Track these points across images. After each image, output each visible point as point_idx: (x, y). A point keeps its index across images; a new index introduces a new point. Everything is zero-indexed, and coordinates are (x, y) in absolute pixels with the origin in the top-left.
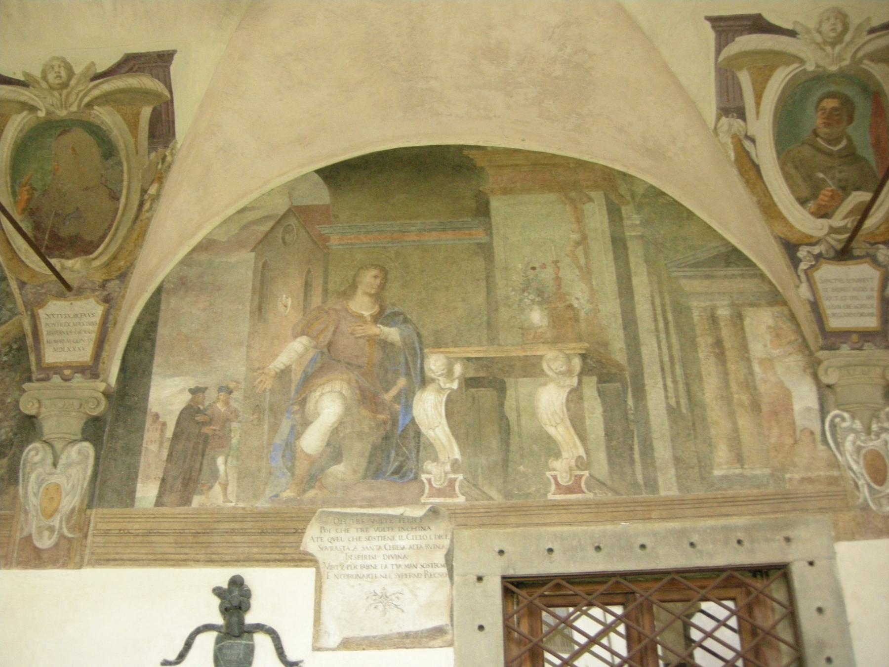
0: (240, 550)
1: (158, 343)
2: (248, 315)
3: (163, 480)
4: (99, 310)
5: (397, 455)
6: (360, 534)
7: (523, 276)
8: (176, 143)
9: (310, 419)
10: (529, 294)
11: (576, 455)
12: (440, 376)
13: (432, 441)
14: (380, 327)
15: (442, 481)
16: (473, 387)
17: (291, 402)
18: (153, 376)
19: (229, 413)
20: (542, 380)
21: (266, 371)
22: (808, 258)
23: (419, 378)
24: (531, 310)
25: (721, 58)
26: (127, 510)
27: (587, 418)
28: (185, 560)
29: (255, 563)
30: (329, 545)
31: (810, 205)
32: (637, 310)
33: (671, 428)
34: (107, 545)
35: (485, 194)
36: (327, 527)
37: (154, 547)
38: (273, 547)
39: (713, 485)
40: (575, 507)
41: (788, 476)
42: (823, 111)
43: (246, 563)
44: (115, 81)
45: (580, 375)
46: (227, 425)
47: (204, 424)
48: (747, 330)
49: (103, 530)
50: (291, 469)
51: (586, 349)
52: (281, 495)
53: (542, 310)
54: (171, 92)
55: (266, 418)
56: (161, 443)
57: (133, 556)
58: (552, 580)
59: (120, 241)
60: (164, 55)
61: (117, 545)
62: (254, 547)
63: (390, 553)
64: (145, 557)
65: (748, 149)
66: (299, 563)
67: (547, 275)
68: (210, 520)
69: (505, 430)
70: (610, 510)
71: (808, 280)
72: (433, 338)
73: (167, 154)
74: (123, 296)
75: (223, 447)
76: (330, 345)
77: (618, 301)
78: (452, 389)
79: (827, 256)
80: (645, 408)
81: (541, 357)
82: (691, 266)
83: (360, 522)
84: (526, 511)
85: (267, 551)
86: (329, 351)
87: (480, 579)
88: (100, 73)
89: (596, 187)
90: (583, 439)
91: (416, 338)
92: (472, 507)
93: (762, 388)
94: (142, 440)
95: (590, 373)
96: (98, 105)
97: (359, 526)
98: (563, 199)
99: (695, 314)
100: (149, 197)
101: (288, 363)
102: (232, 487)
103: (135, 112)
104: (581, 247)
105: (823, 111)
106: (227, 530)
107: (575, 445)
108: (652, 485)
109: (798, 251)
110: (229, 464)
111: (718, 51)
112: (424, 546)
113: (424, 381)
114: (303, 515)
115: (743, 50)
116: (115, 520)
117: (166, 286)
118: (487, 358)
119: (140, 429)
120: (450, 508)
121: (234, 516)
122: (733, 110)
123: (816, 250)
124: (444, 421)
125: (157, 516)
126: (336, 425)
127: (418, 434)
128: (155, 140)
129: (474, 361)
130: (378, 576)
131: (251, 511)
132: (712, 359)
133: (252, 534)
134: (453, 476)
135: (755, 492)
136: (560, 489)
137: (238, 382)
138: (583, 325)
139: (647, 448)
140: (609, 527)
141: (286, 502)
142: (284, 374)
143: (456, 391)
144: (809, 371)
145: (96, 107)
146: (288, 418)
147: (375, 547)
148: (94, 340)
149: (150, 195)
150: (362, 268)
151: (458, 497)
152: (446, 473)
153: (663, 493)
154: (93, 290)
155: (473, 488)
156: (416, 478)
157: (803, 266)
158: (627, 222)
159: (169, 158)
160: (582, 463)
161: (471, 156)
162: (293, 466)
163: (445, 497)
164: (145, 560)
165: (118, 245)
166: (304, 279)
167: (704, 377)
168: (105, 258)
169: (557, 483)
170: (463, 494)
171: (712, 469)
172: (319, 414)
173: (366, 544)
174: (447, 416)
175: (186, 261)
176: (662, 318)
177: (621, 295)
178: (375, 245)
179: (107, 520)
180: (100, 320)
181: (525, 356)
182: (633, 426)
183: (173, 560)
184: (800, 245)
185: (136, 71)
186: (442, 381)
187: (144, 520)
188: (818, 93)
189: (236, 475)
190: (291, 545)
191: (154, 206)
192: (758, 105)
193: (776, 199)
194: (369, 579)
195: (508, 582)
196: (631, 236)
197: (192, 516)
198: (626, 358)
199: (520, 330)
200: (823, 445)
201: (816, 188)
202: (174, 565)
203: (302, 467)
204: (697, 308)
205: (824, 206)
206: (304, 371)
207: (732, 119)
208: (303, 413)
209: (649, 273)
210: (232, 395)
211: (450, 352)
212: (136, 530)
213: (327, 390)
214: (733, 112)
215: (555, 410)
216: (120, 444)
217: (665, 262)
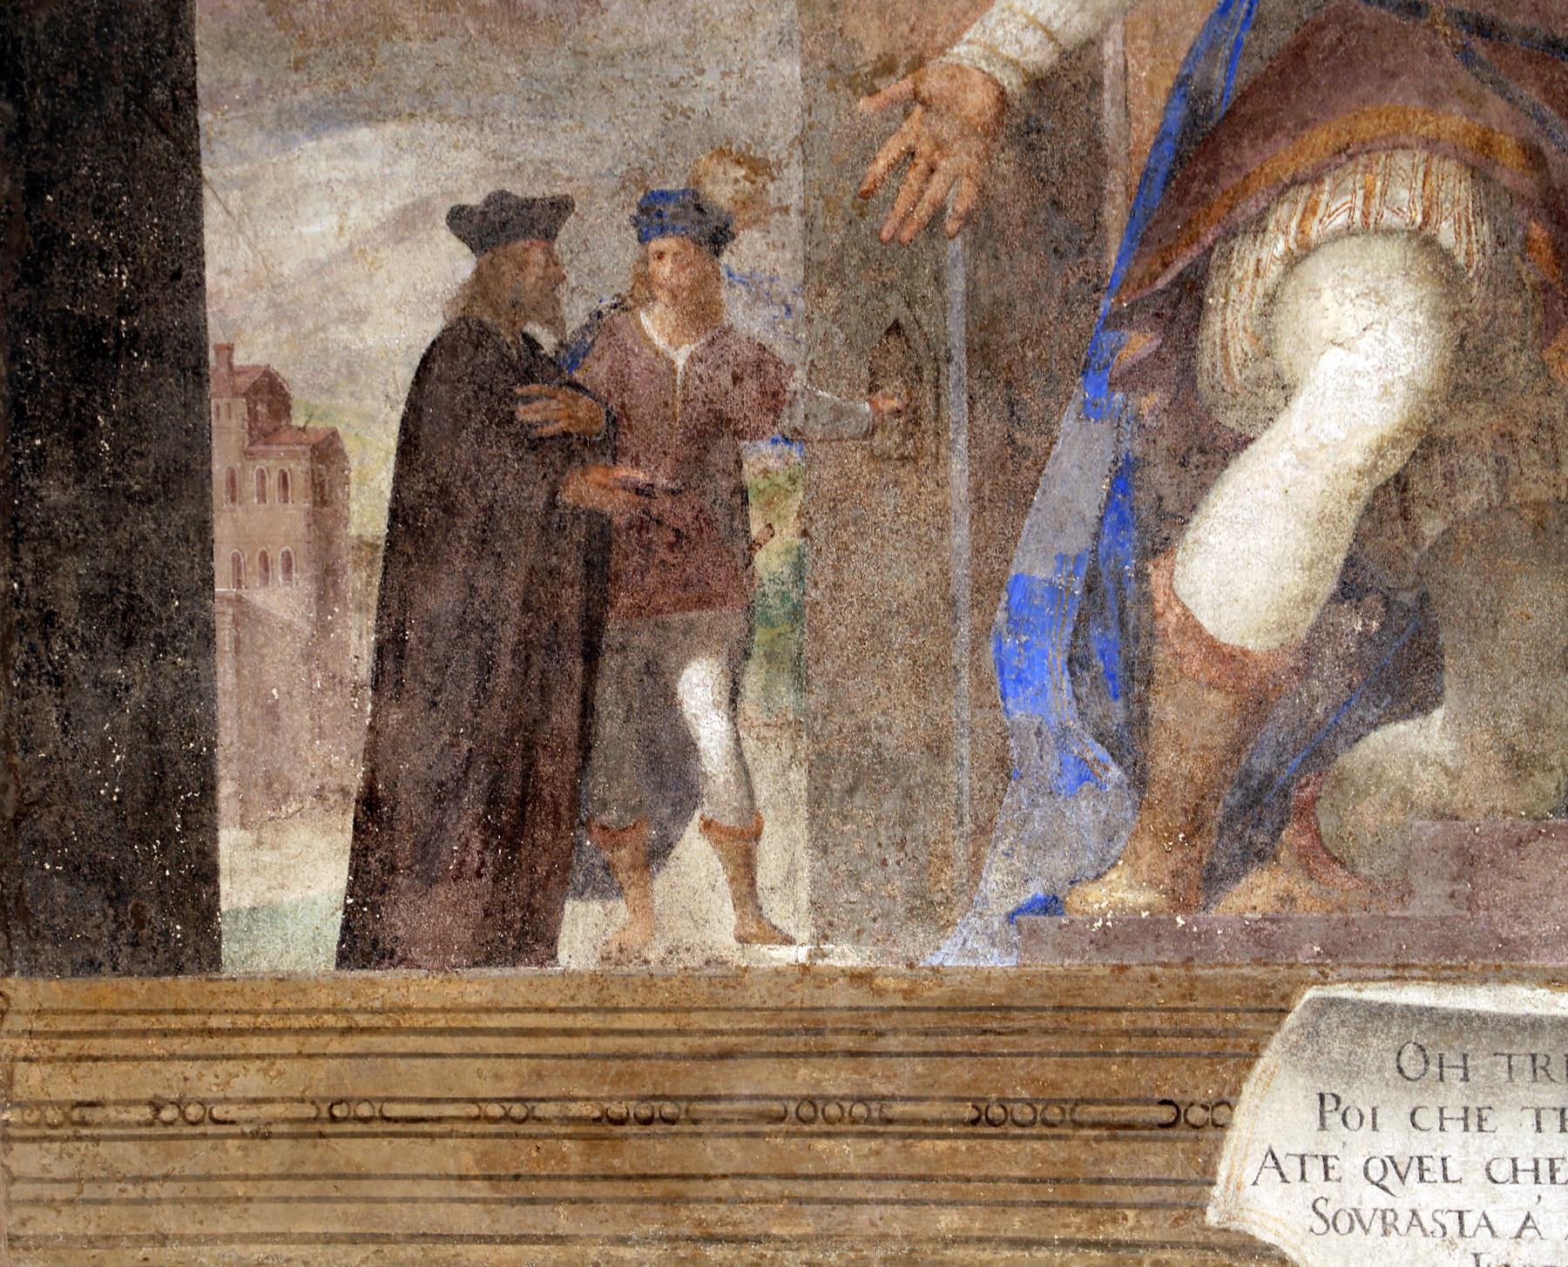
0: (863, 1217)
9: (1230, 419)
17: (1106, 303)
19: (725, 379)
21: (933, 83)
30: (1373, 1199)
34: (90, 1191)
36: (1359, 1098)
37: (368, 1200)
38: (1046, 1204)
46: (718, 457)
49: (59, 1105)
52: (1074, 901)
55: (956, 410)
56: (327, 578)
61: (153, 1189)
62: (939, 1203)
68: (678, 1045)
75: (704, 602)
94: (208, 552)
101: (1076, 26)
106: (777, 1107)
110: (750, 706)
114: (1211, 1021)
116: (118, 1045)
125: (362, 1020)
131: (907, 994)
133: (916, 1129)
137: (758, 167)
141: (1105, 941)
146: (1090, 411)
162: (1140, 722)
172: (1287, 390)
179: (67, 1047)
187: (289, 1044)
189: (798, 778)
190: (1150, 1194)
197: (568, 1021)
206: (1182, 82)
208: (1188, 374)
210: (725, 258)
212: (256, 1101)
213: (1340, 220)
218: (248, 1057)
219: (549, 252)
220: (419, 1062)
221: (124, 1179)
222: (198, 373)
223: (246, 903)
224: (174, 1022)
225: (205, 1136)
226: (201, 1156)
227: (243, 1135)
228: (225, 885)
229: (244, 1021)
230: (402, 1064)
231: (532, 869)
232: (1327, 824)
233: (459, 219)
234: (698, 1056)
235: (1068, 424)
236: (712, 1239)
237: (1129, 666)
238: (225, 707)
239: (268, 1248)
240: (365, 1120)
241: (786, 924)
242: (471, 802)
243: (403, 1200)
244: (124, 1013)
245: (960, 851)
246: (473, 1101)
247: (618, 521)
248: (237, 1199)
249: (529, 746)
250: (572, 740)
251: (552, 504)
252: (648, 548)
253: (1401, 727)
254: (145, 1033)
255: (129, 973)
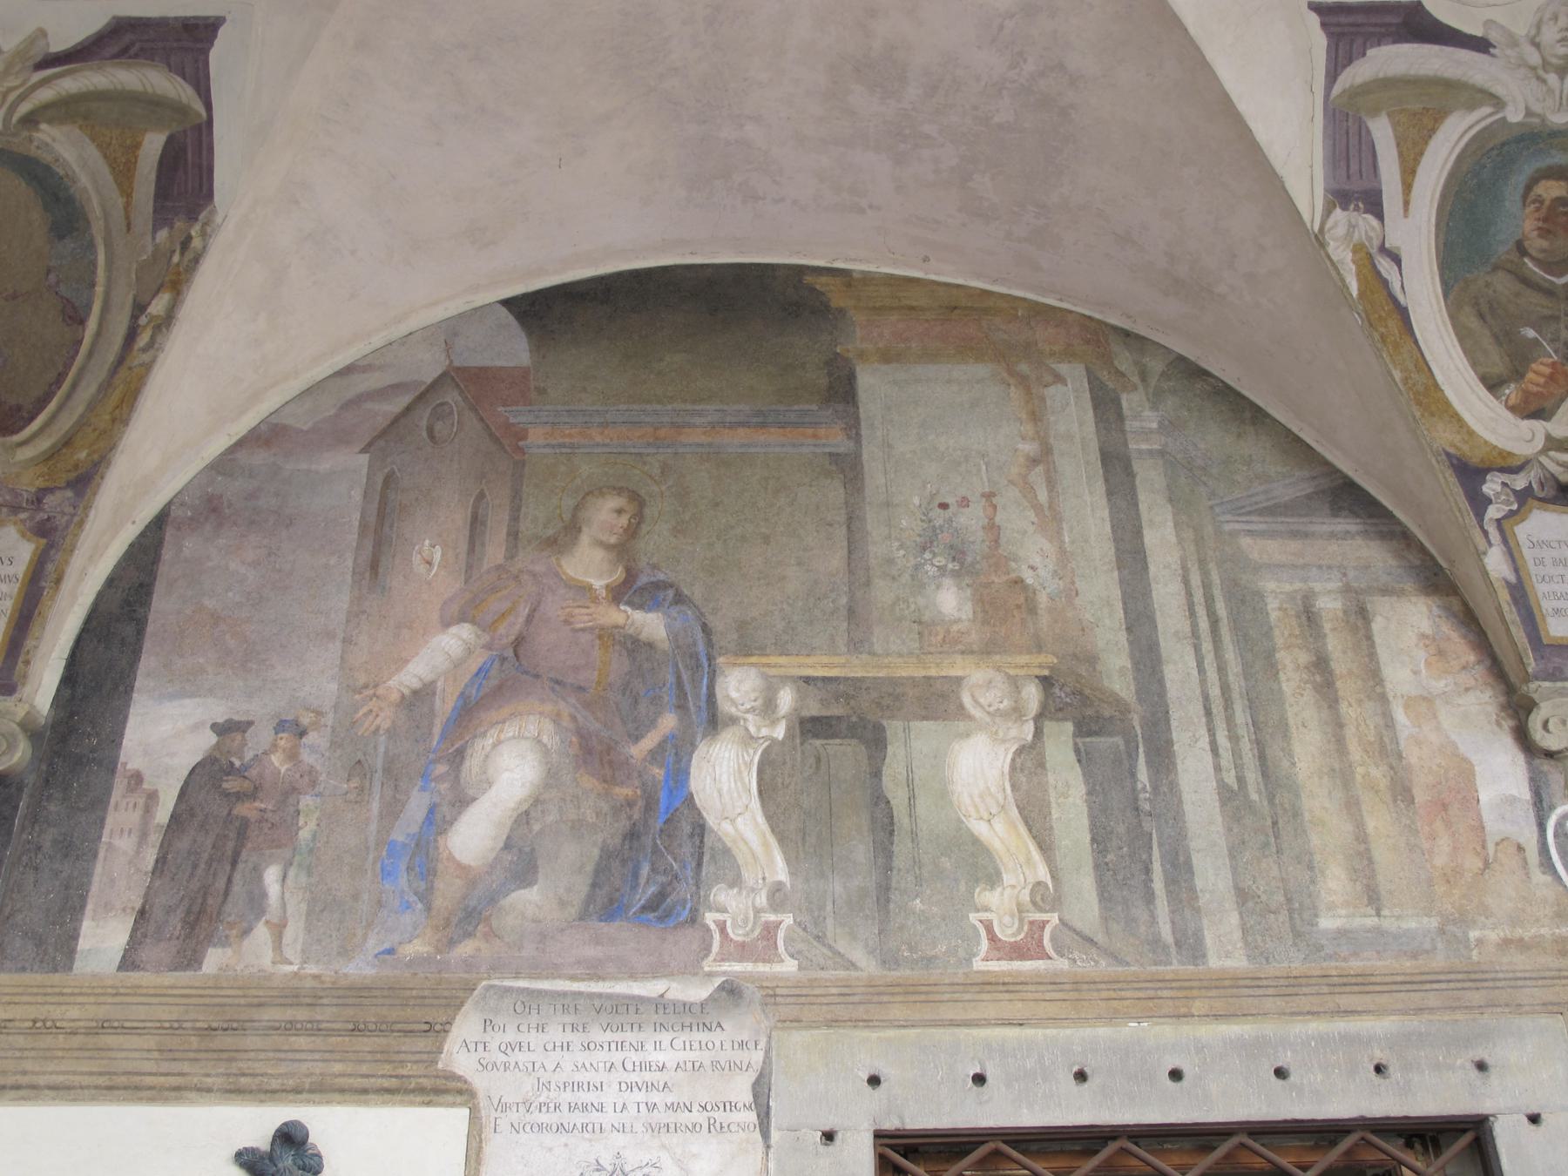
0: (304, 1067)
1: (150, 628)
2: (349, 578)
3: (142, 913)
4: (24, 552)
5: (654, 870)
6: (569, 1036)
7: (922, 521)
8: (213, 212)
9: (471, 792)
10: (935, 555)
11: (1031, 880)
12: (748, 711)
13: (729, 844)
14: (625, 612)
15: (750, 925)
16: (816, 736)
17: (431, 756)
18: (135, 695)
19: (298, 776)
20: (961, 726)
21: (380, 691)
22: (1503, 497)
23: (704, 715)
24: (938, 587)
25: (1337, 89)
26: (56, 978)
27: (1054, 805)
28: (178, 1089)
29: (337, 1096)
30: (502, 1058)
31: (1507, 391)
32: (1154, 593)
33: (1230, 830)
35: (847, 360)
36: (499, 1021)
37: (110, 1058)
38: (376, 1061)
39: (1320, 948)
40: (1030, 988)
41: (1474, 934)
42: (1537, 205)
43: (316, 1097)
44: (87, 73)
45: (1039, 718)
46: (291, 800)
47: (240, 796)
48: (1378, 640)
50: (426, 897)
51: (1052, 668)
52: (400, 950)
53: (960, 588)
54: (209, 106)
56: (144, 836)
57: (60, 1079)
58: (983, 1143)
59: (81, 409)
60: (196, 26)
61: (26, 1053)
62: (335, 1061)
63: (634, 1077)
64: (86, 1080)
65: (1385, 274)
66: (432, 1097)
67: (971, 520)
68: (242, 1001)
69: (884, 827)
70: (1104, 994)
71: (1505, 541)
72: (735, 636)
73: (193, 233)
74: (81, 524)
76: (518, 643)
77: (1116, 574)
78: (774, 741)
79: (1541, 495)
80: (1174, 787)
81: (959, 680)
82: (1261, 512)
83: (572, 1010)
84: (927, 993)
85: (364, 1069)
86: (516, 655)
87: (829, 1136)
88: (55, 54)
89: (1068, 354)
90: (1046, 847)
91: (700, 635)
92: (812, 983)
93: (1413, 756)
94: (102, 827)
95: (1060, 715)
96: (50, 122)
97: (568, 1019)
98: (1005, 375)
99: (1272, 604)
100: (149, 322)
101: (429, 677)
102: (294, 932)
103: (128, 142)
104: (1040, 469)
105: (1537, 205)
106: (277, 1025)
107: (1029, 860)
108: (1190, 945)
109: (1484, 482)
110: (289, 882)
111: (1332, 76)
112: (707, 1063)
113: (714, 722)
114: (446, 993)
115: (1381, 75)
116: (25, 999)
117: (176, 512)
118: (846, 679)
119: (100, 803)
120: (765, 984)
121: (291, 995)
122: (1356, 195)
123: (1520, 482)
124: (755, 804)
125: (122, 991)
126: (525, 807)
127: (700, 829)
128: (169, 204)
129: (820, 684)
130: (607, 1127)
131: (334, 983)
132: (1309, 695)
133: (331, 1032)
134: (772, 917)
135: (1408, 964)
136: (998, 949)
137: (319, 713)
138: (1044, 620)
139: (1180, 870)
140: (1103, 1032)
142: (421, 696)
143: (783, 743)
144: (1508, 724)
145: (43, 126)
147: (601, 1065)
148: (9, 612)
149: (152, 318)
150: (588, 494)
151: (782, 961)
152: (757, 911)
153: (1214, 962)
154: (15, 509)
155: (815, 943)
156: (694, 919)
157: (1493, 512)
158: (1131, 425)
159: (196, 243)
160: (1047, 899)
161: (818, 287)
162: (430, 889)
163: (756, 961)
164: (88, 1087)
165: (75, 417)
166: (470, 510)
167: (1293, 730)
168: (44, 444)
169: (992, 937)
170: (792, 956)
171: (1316, 916)
172: (490, 784)
173: (581, 1057)
174: (760, 792)
175: (223, 465)
176: (1205, 612)
177: (1120, 564)
178: (622, 450)
180: (25, 575)
181: (924, 677)
182: (1148, 825)
183: (151, 1088)
184: (1488, 470)
185: (136, 56)
186: (752, 723)
187: (92, 999)
188: (1529, 169)
189: (304, 906)
190: (417, 1057)
191: (159, 339)
192: (1407, 187)
193: (1439, 378)
194: (587, 1135)
195: (887, 1146)
196: (1140, 452)
198: (1133, 688)
199: (916, 626)
200: (1544, 873)
201: (1519, 359)
202: (151, 1100)
203: (447, 891)
204: (1276, 591)
205: (1536, 394)
206: (462, 694)
207: (1356, 213)
208: (457, 778)
209: (1176, 525)
210: (304, 740)
211: (768, 665)
212: (74, 1020)
213: (511, 734)
214: (1357, 199)
215: (988, 788)
216: (48, 837)
217: (1210, 503)
218: (75, 1004)
219: (243, 737)
220: (140, 1007)
221: (16, 1049)
222: (113, 771)
223: (88, 947)
224: (49, 990)
225: (51, 1033)
226: (48, 1041)
227: (66, 1033)
228: (81, 941)
229: (76, 991)
230: (134, 1007)
231: (198, 937)
232: (494, 923)
233: (214, 727)
234: (251, 1005)
235: (415, 792)
236: (244, 1075)
237: (428, 871)
238: (96, 879)
239: (66, 1077)
240: (116, 1028)
241: (292, 959)
242: (180, 913)
243: (125, 1059)
244: (31, 987)
245: (360, 932)
246: (159, 1021)
247: (253, 820)
248: (58, 1058)
249: (205, 894)
250: (222, 892)
251: (229, 814)
252: (261, 829)
253: (522, 891)
254: (37, 994)
255: (37, 972)
